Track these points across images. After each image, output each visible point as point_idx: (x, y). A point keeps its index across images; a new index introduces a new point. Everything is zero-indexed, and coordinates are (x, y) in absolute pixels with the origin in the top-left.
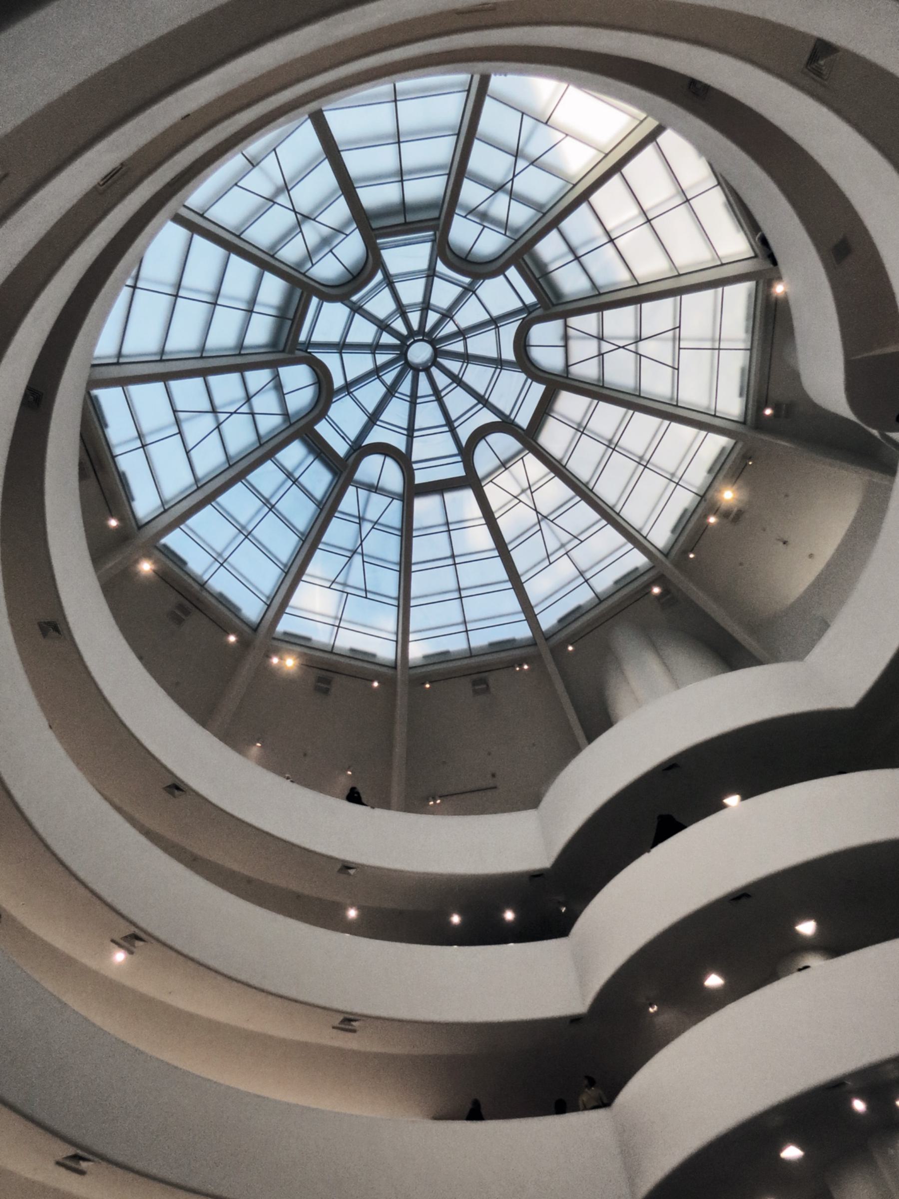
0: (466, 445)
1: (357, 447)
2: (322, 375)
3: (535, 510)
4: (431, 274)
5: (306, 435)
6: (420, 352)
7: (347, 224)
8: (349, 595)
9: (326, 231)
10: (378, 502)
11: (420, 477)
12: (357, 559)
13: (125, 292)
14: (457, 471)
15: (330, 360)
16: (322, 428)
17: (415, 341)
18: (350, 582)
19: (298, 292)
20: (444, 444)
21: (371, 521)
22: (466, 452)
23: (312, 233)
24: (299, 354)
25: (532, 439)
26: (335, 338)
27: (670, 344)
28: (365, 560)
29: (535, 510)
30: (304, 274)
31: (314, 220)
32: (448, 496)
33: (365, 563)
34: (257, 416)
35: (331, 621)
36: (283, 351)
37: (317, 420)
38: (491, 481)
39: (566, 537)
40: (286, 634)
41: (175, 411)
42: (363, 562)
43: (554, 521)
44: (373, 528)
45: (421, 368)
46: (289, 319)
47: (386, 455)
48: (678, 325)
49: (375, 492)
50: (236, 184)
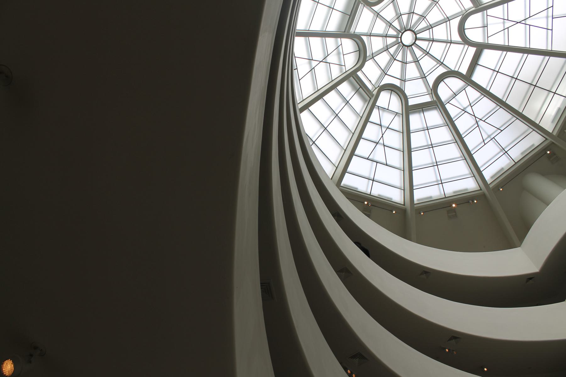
0: (462, 39)
1: (431, 91)
2: (391, 88)
4: (378, 15)
5: (410, 110)
6: (407, 38)
7: (337, 42)
10: (462, 97)
11: (464, 70)
12: (481, 123)
13: (313, 147)
14: (472, 51)
15: (387, 80)
16: (411, 102)
17: (401, 38)
18: (489, 134)
19: (351, 78)
20: (456, 50)
22: (466, 41)
23: (332, 59)
24: (375, 93)
25: (480, 5)
26: (378, 72)
30: (346, 72)
31: (328, 55)
32: (480, 62)
34: (389, 127)
35: (502, 153)
36: (370, 99)
38: (488, 37)
40: (492, 177)
41: (367, 159)
42: (484, 121)
44: (471, 107)
45: (414, 41)
46: (360, 88)
47: (442, 80)
49: (456, 95)
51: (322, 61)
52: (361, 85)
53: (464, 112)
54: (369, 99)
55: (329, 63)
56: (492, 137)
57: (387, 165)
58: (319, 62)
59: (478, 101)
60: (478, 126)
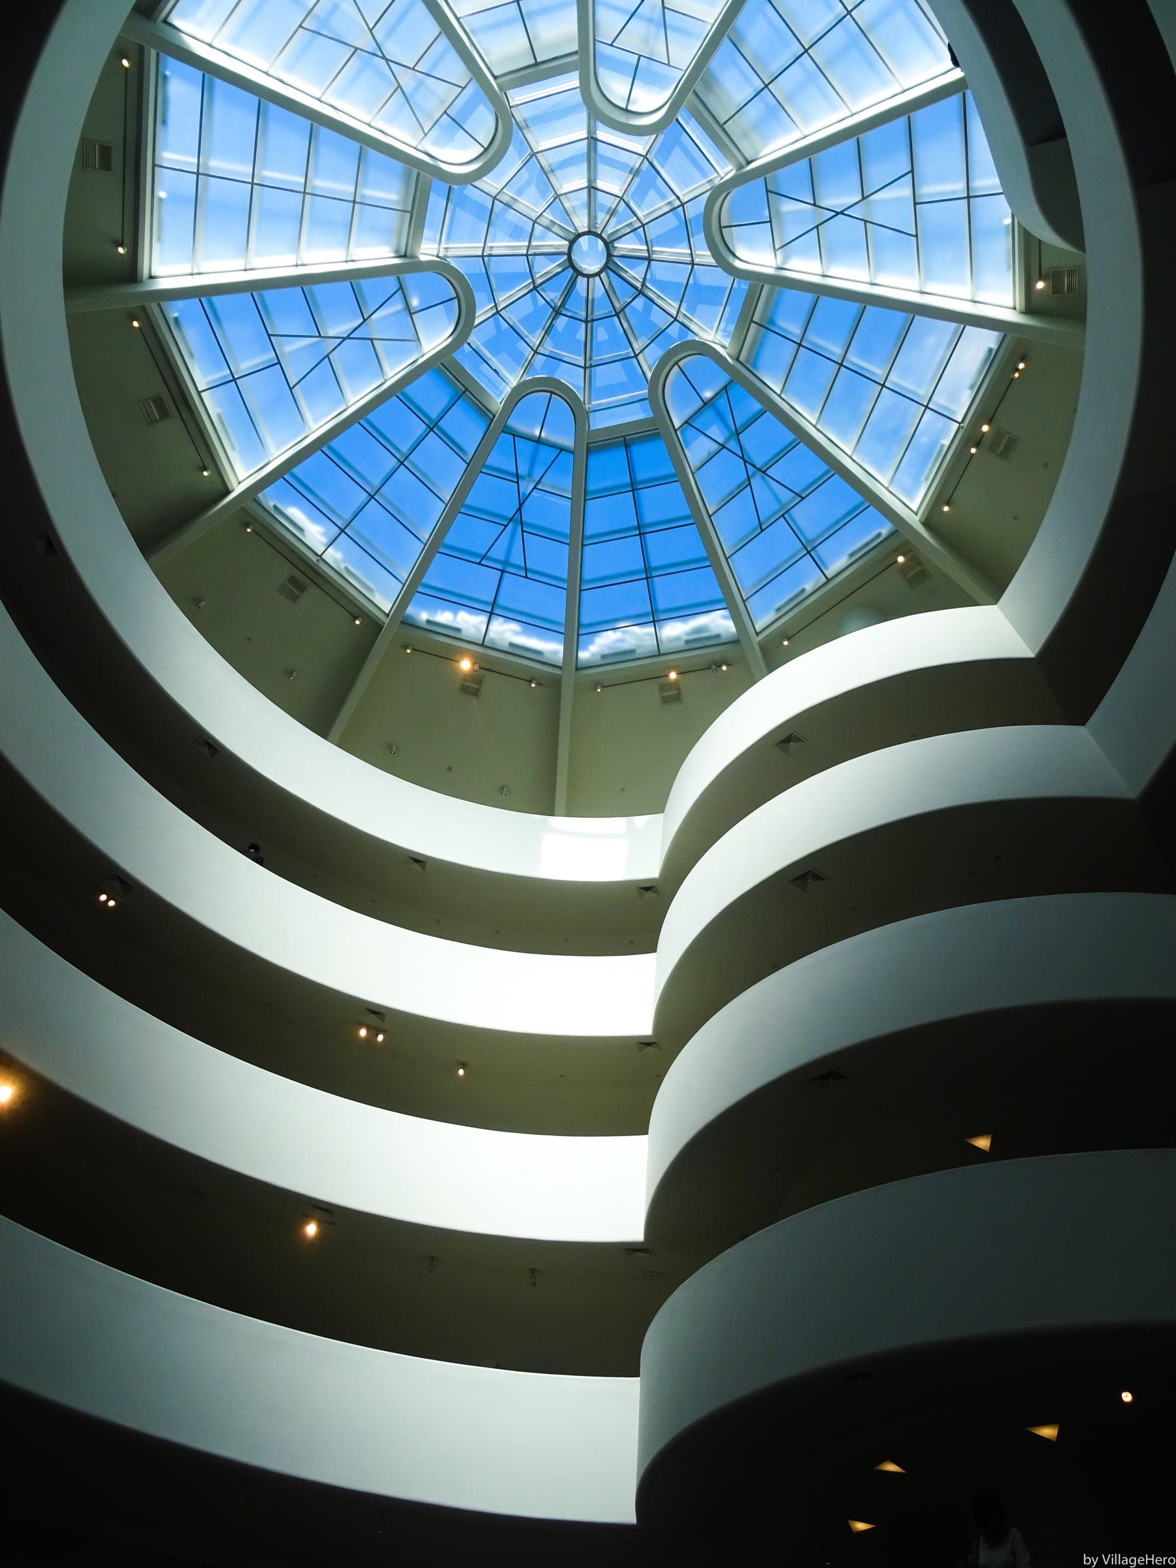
3: (521, 505)
27: (776, 507)
29: (521, 505)
39: (516, 558)
43: (524, 533)
48: (803, 496)
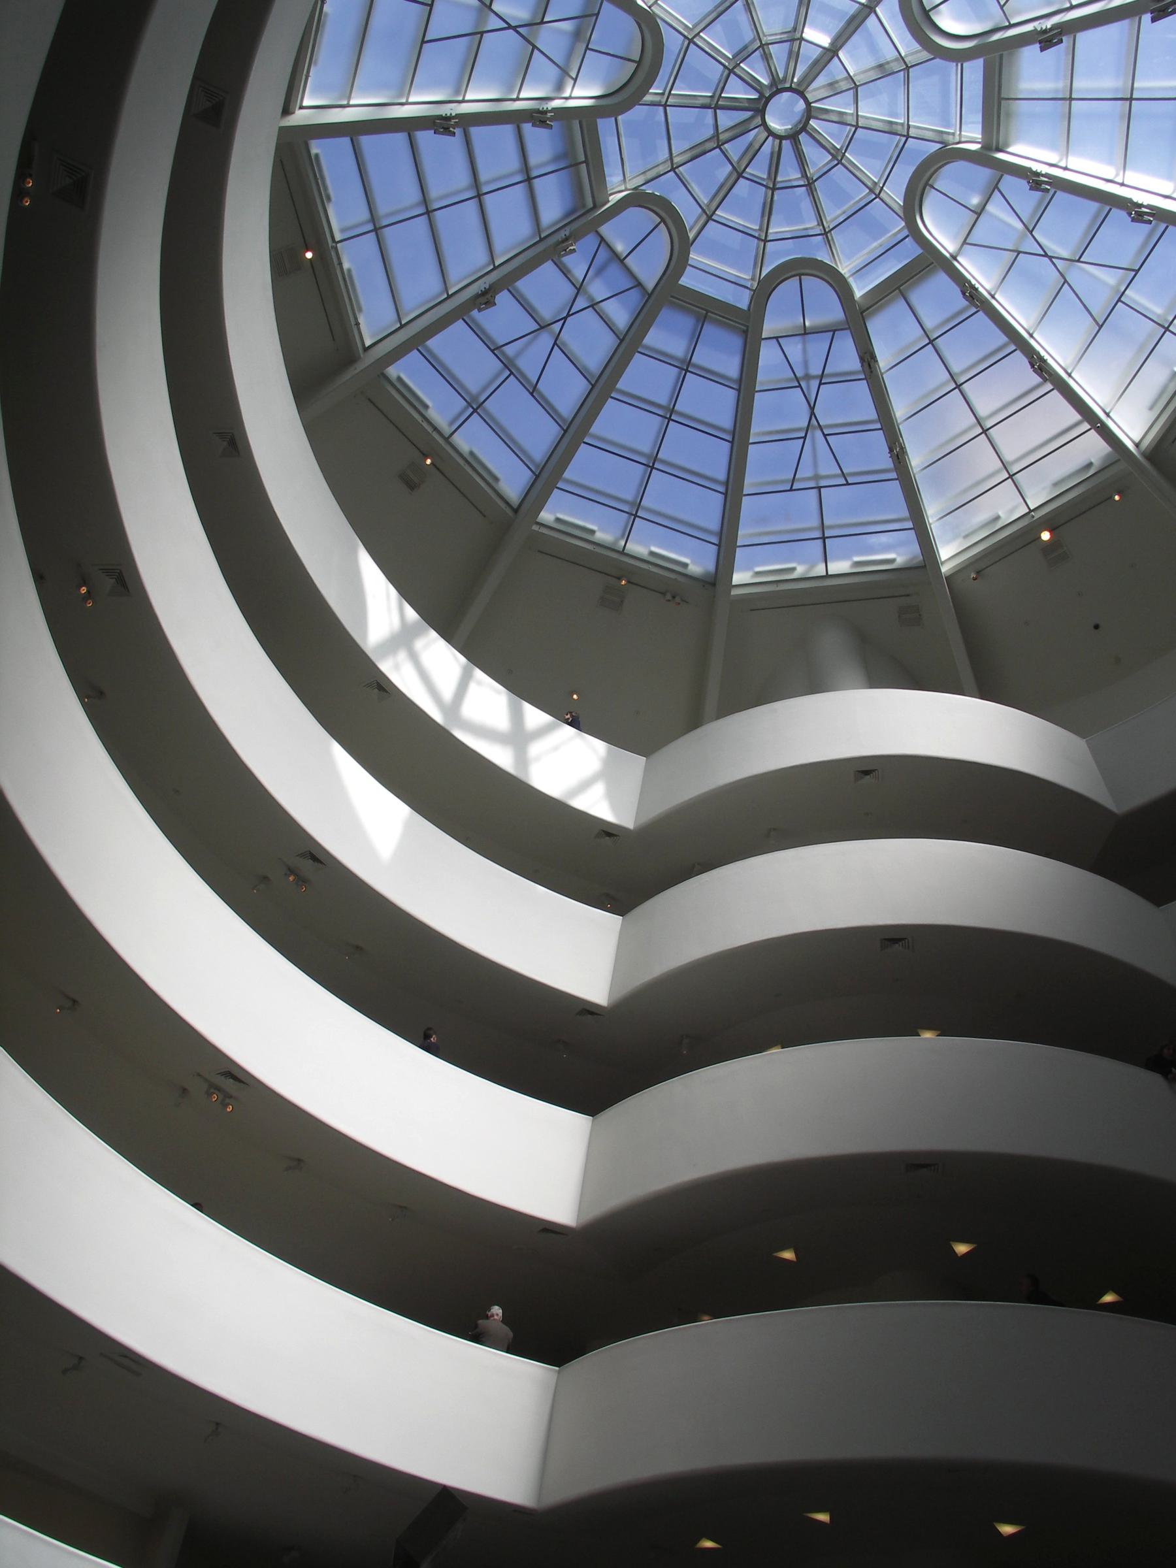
8: (822, 489)
9: (567, 26)
10: (818, 346)
21: (814, 377)
28: (826, 433)
33: (828, 437)
37: (680, 273)
41: (495, 349)
42: (825, 436)
44: (820, 384)
46: (582, 162)
50: (423, 42)
51: (515, 28)
52: (589, 157)
53: (797, 385)
54: (592, 206)
55: (534, 47)
56: (822, 483)
57: (533, 391)
58: (505, 25)
59: (845, 378)
60: (805, 438)
